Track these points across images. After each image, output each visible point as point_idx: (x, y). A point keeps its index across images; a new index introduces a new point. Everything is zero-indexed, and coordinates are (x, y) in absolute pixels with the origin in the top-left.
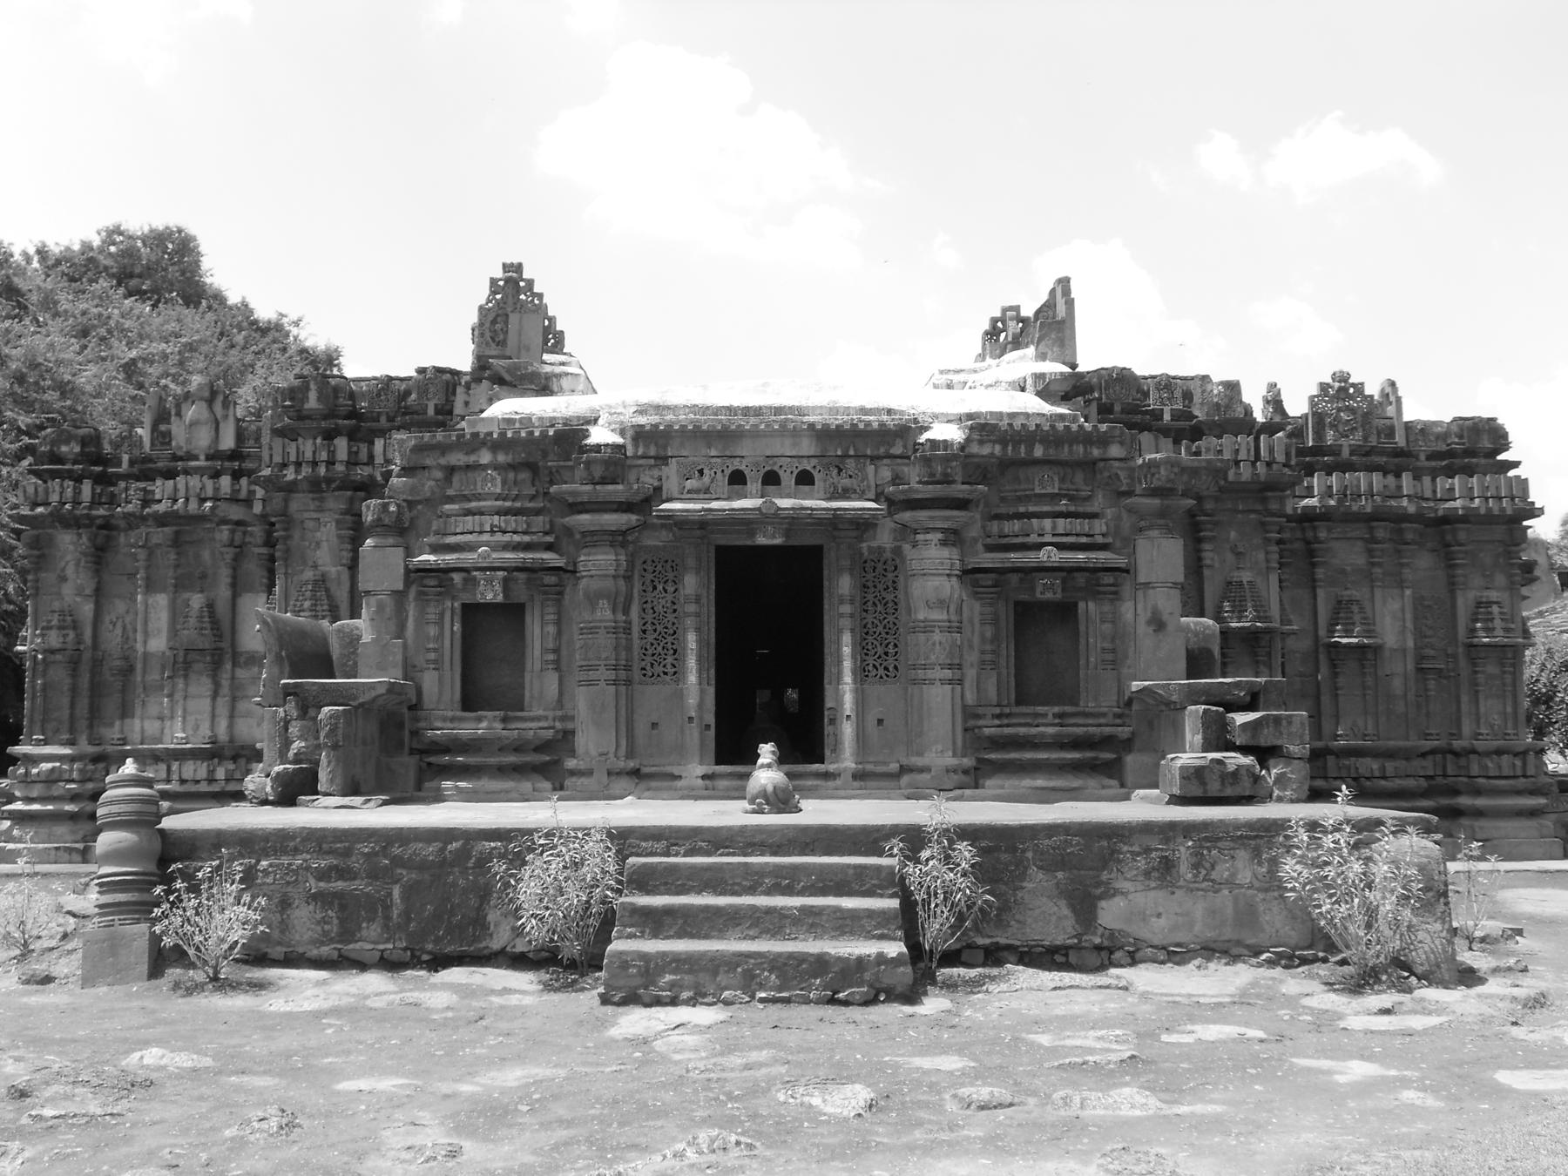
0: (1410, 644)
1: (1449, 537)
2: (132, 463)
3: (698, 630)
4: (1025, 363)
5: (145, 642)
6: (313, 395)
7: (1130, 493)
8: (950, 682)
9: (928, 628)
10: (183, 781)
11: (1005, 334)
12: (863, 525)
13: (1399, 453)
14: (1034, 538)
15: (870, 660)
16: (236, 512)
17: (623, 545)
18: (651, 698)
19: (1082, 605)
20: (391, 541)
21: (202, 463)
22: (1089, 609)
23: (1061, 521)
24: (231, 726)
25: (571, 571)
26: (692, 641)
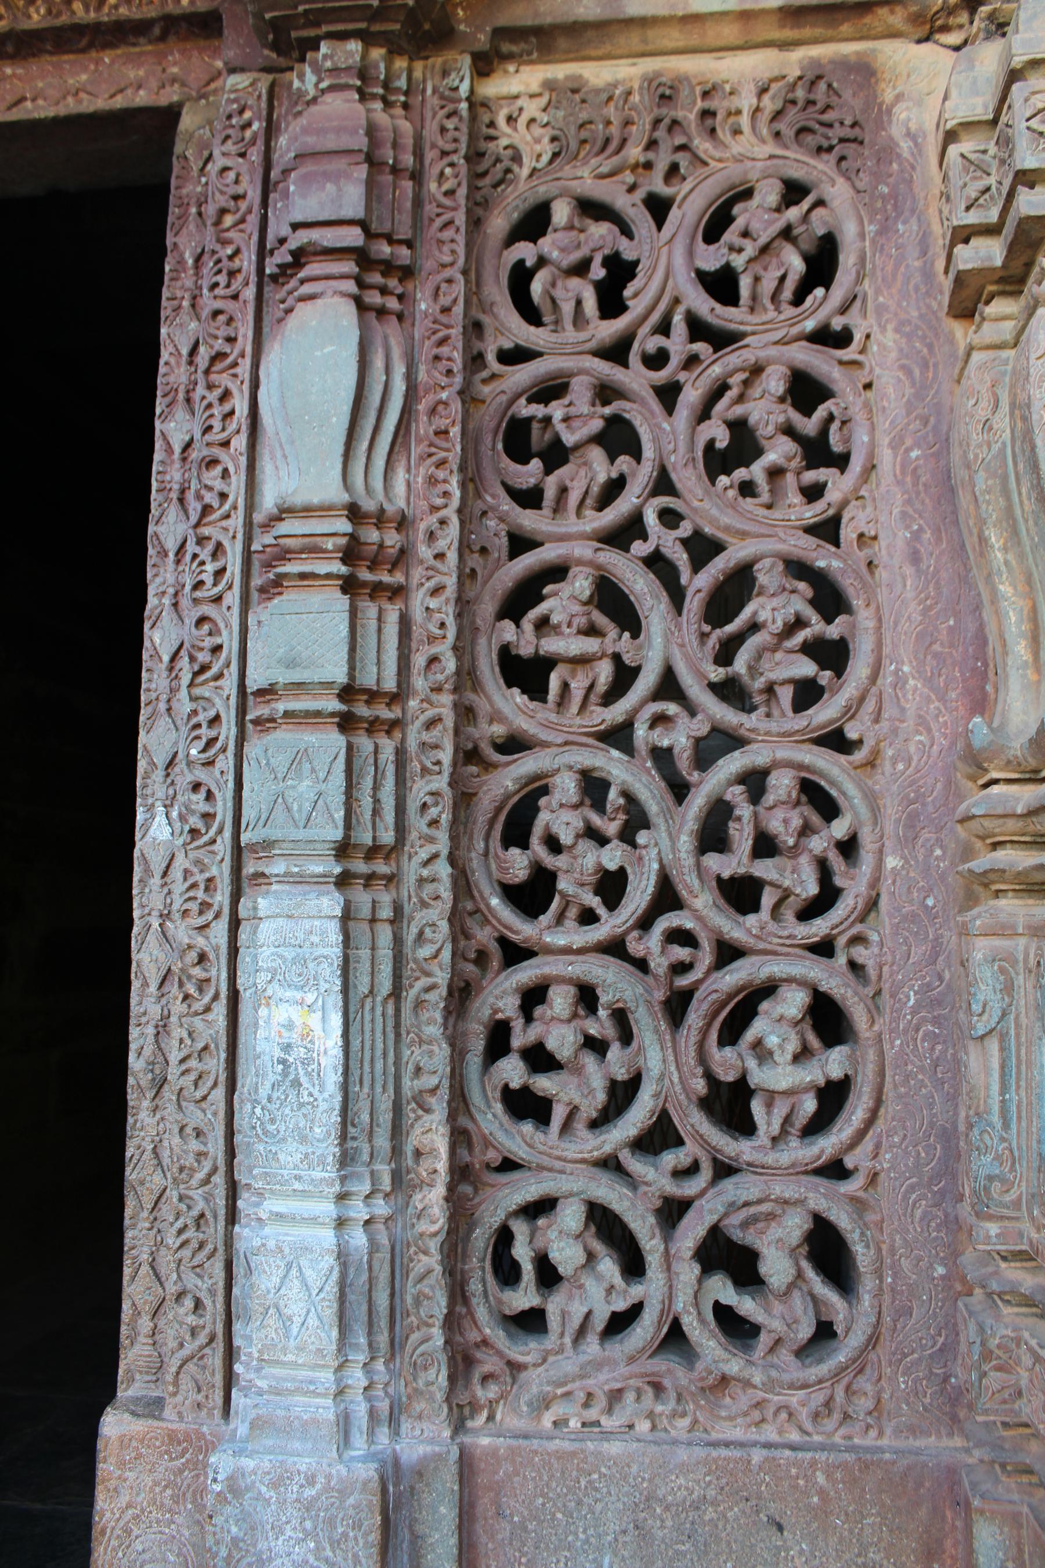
15: (564, 1164)
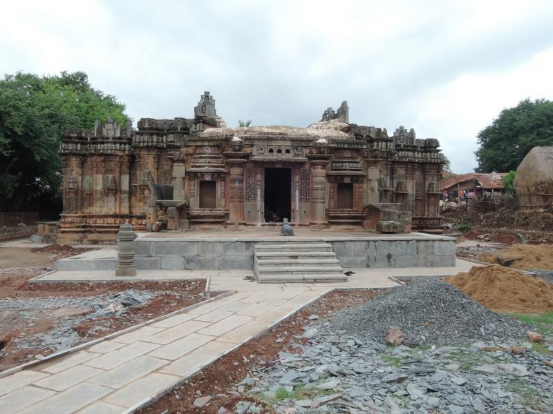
0: (414, 193)
1: (425, 167)
2: (91, 139)
3: (260, 189)
4: (336, 123)
6: (147, 124)
7: (367, 157)
8: (322, 203)
9: (317, 189)
11: (329, 116)
12: (302, 164)
13: (414, 147)
14: (344, 168)
16: (120, 153)
17: (242, 167)
18: (248, 206)
19: (354, 185)
20: (182, 164)
21: (111, 140)
22: (356, 185)
23: (351, 164)
24: (120, 209)
25: (228, 174)
26: (259, 193)
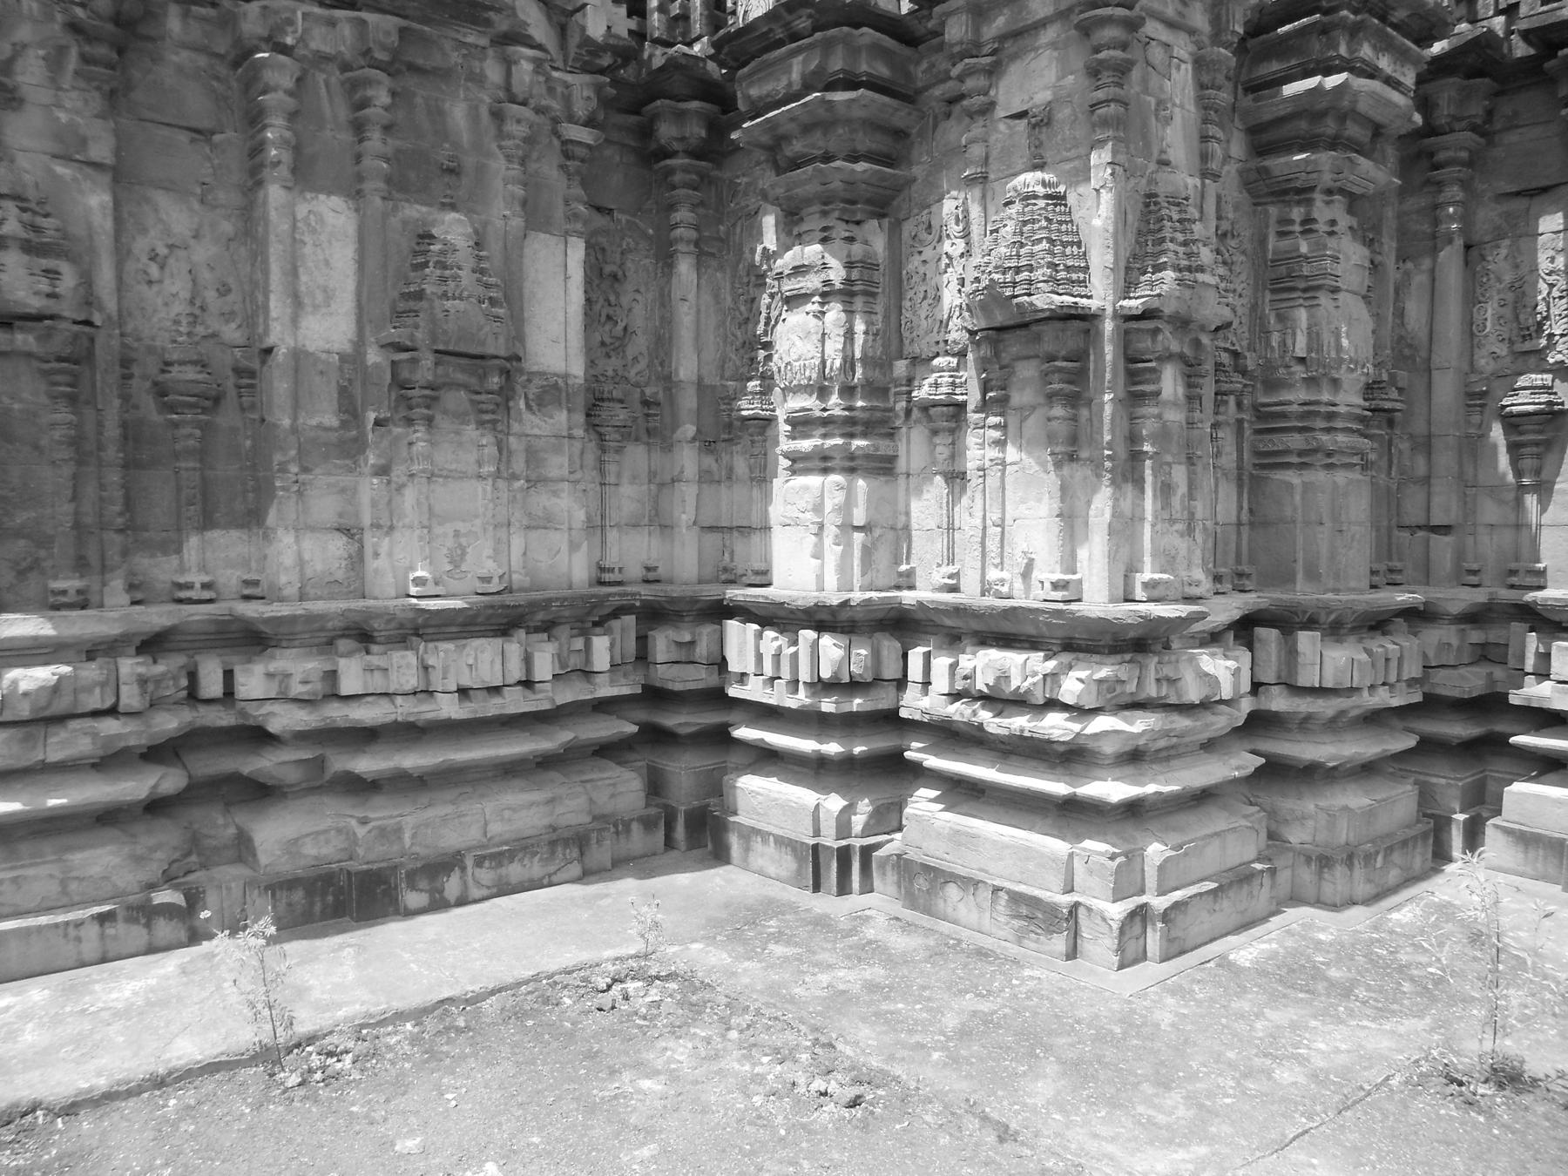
5: (295, 321)
10: (463, 692)
